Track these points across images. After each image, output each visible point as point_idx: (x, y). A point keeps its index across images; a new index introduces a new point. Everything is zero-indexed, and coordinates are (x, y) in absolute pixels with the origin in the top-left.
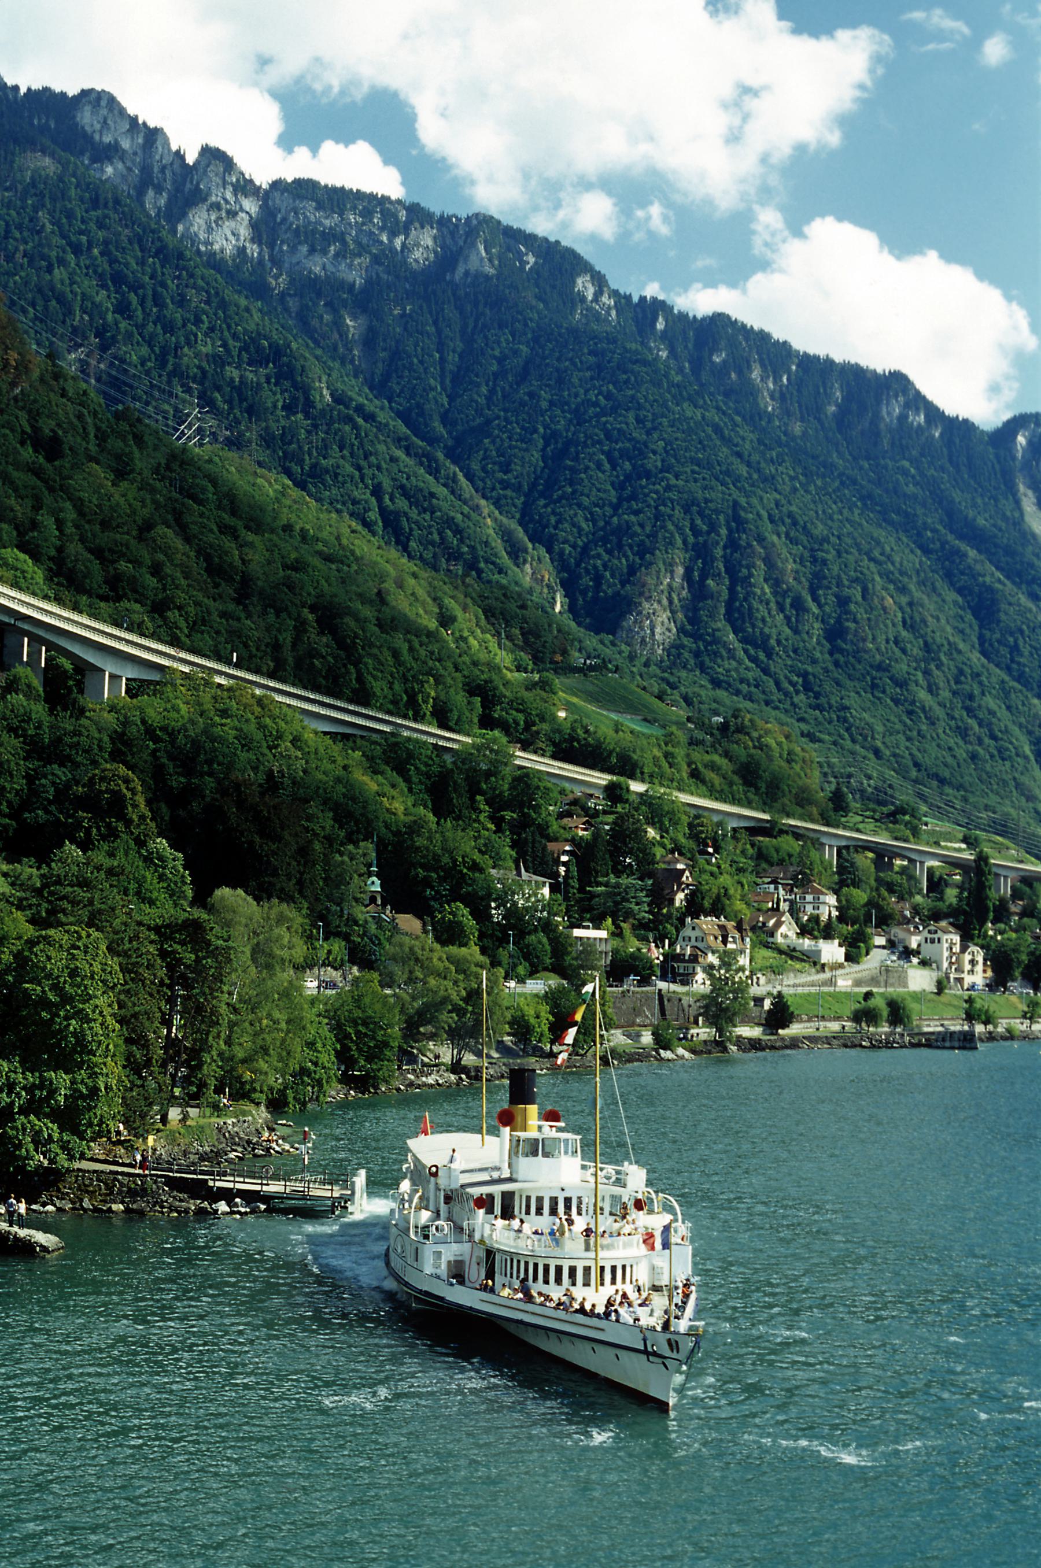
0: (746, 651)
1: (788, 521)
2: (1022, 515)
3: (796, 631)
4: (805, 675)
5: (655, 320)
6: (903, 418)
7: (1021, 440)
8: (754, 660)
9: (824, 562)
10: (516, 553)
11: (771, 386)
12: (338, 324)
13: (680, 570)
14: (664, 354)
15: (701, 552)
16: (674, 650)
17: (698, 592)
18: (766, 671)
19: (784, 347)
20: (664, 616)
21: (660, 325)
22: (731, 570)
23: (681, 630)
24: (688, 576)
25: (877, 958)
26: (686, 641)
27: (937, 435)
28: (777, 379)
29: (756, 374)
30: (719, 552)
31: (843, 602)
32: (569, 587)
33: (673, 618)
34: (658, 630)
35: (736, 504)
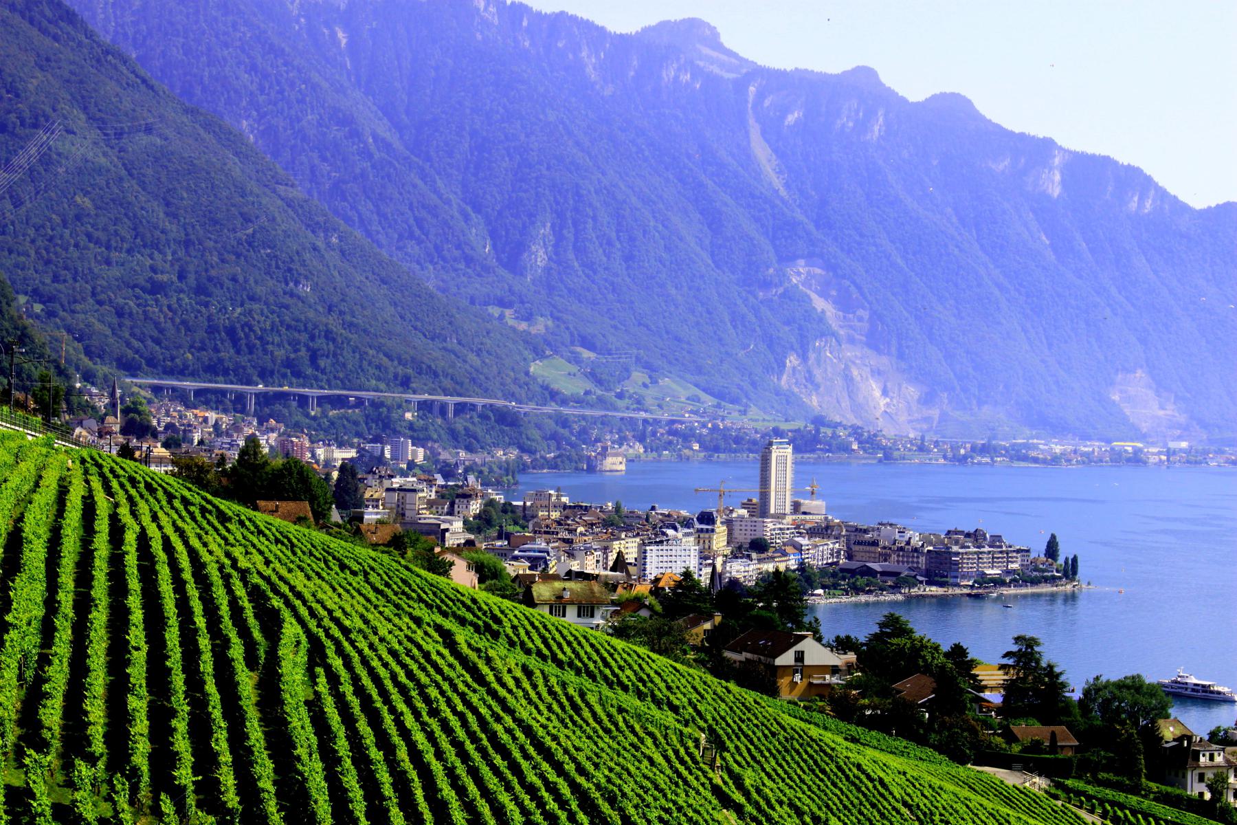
0: (583, 271)
1: (605, 192)
2: (749, 142)
3: (609, 258)
4: (612, 284)
5: (521, 20)
6: (676, 78)
7: (752, 89)
8: (588, 276)
9: (623, 217)
10: (466, 218)
11: (594, 60)
12: (333, 35)
13: (549, 225)
14: (527, 44)
15: (560, 215)
16: (547, 270)
17: (559, 238)
18: (593, 282)
19: (601, 31)
20: (541, 253)
21: (525, 23)
22: (575, 224)
23: (550, 259)
24: (553, 226)
25: (625, 447)
26: (553, 265)
27: (698, 86)
28: (598, 57)
29: (584, 54)
30: (569, 214)
31: (632, 239)
32: (493, 235)
33: (546, 253)
34: (539, 260)
35: (577, 185)
